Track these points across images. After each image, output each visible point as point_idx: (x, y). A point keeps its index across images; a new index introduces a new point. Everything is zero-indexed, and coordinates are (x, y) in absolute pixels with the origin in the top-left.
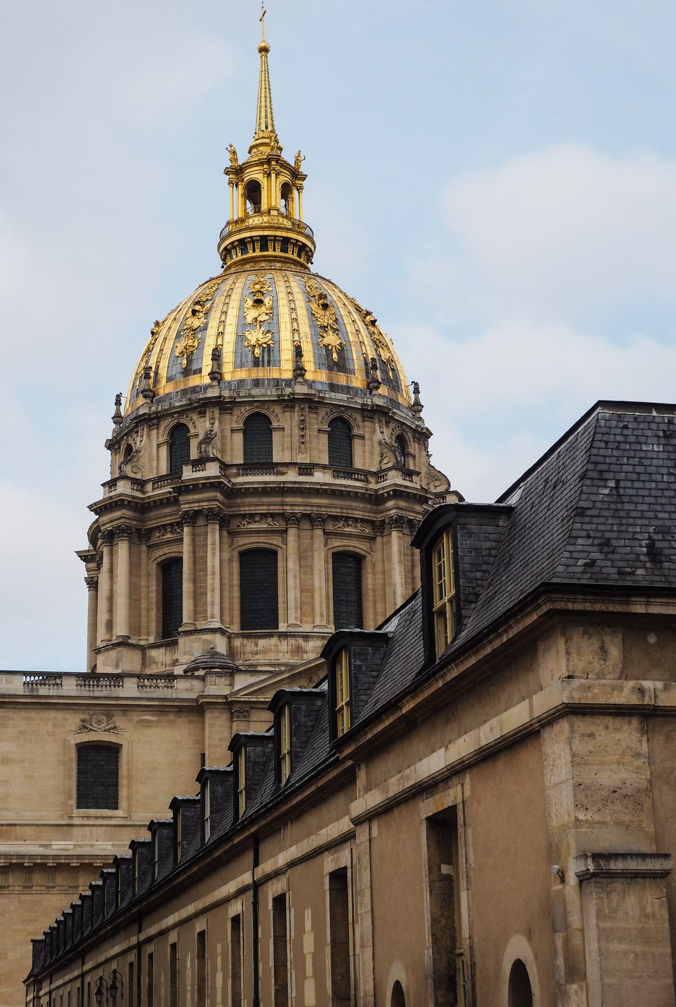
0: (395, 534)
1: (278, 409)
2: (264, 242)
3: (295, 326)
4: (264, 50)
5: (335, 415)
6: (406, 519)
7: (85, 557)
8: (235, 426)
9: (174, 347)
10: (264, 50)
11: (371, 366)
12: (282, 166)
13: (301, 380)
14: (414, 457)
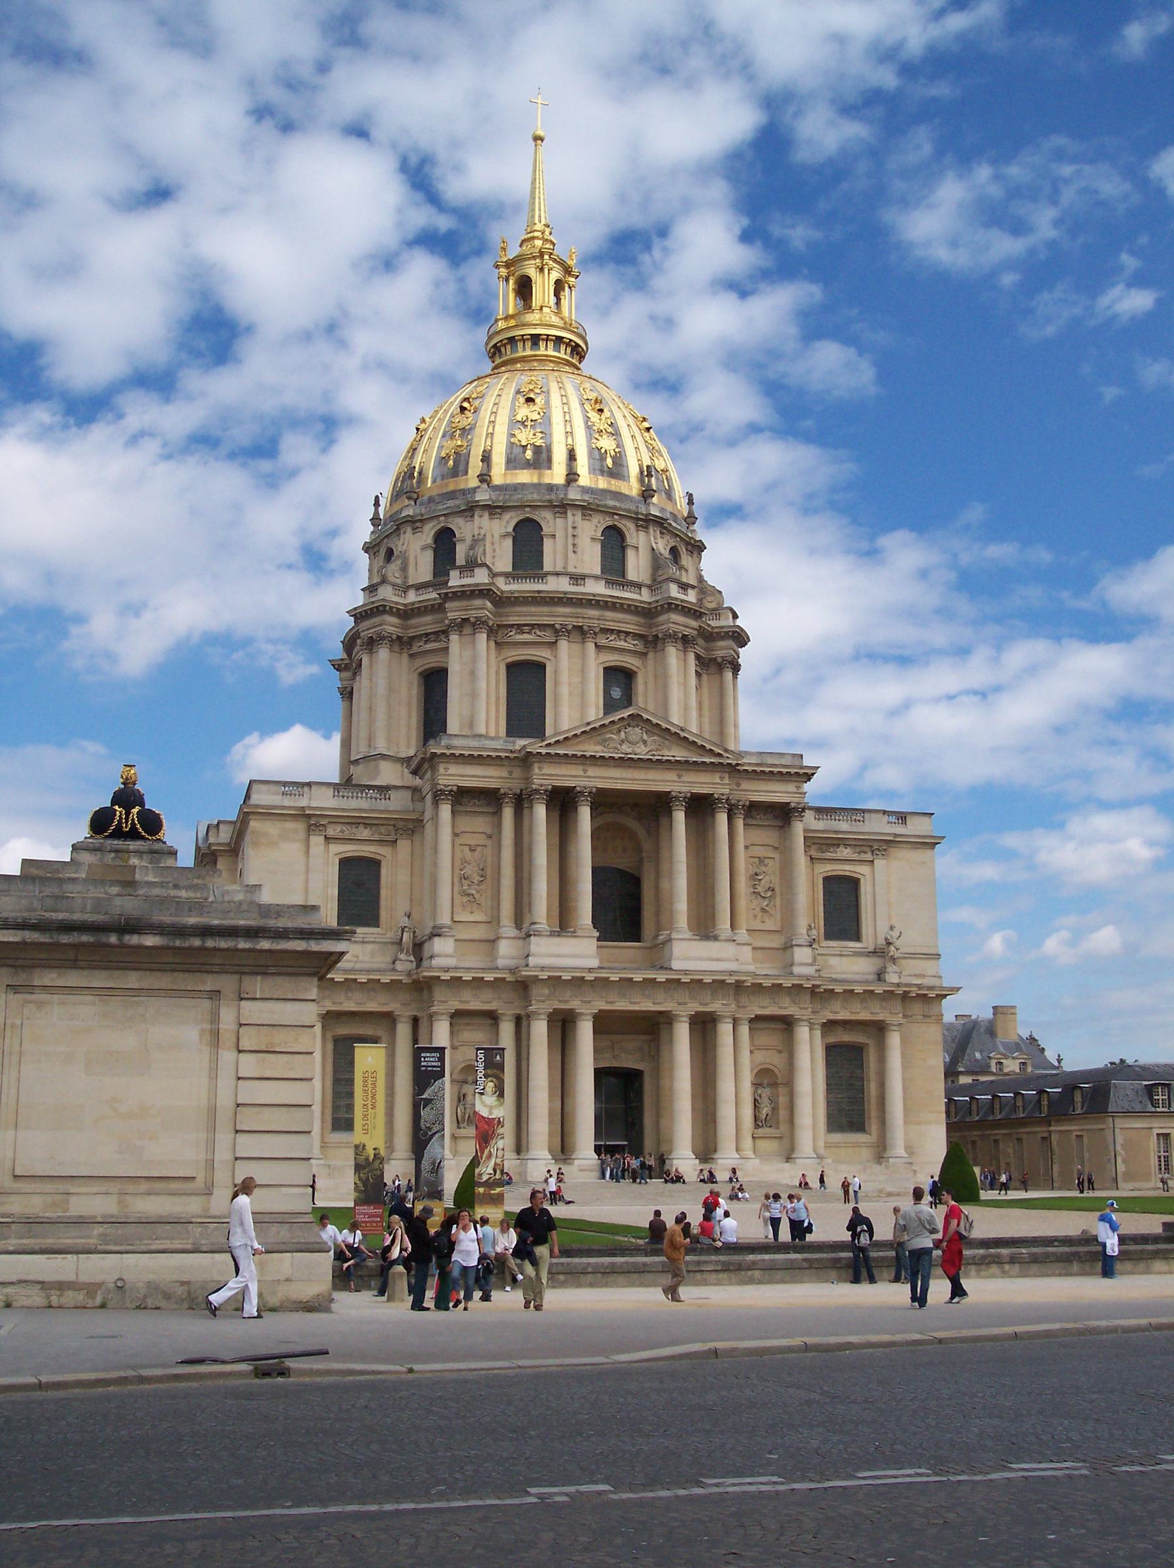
2: (535, 339)
3: (569, 429)
5: (610, 523)
7: (339, 666)
8: (503, 531)
9: (441, 447)
12: (555, 261)
14: (687, 571)
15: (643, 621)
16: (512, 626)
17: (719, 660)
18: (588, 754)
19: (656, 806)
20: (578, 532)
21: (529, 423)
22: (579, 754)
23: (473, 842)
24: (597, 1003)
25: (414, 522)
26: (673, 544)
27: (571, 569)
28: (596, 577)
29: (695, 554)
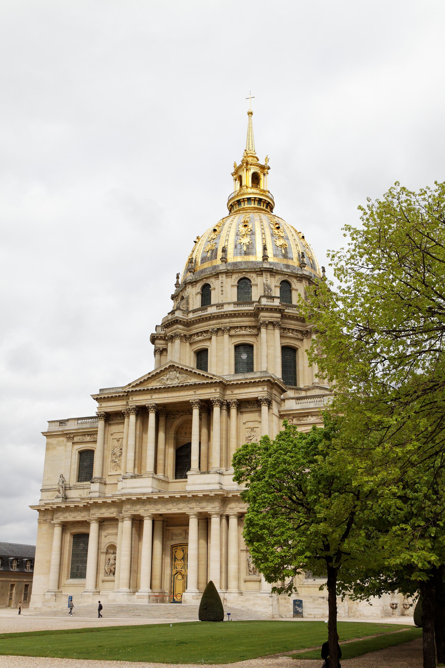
0: (263, 330)
1: (213, 280)
2: (239, 202)
4: (250, 113)
5: (242, 276)
6: (267, 322)
10: (250, 113)
11: (265, 249)
12: (251, 165)
13: (224, 263)
15: (253, 319)
16: (194, 334)
17: (309, 330)
18: (149, 388)
19: (185, 408)
20: (224, 284)
21: (212, 240)
22: (146, 388)
23: (118, 437)
24: (151, 511)
25: (176, 297)
26: (285, 279)
27: (220, 302)
28: (229, 303)
29: (304, 282)
